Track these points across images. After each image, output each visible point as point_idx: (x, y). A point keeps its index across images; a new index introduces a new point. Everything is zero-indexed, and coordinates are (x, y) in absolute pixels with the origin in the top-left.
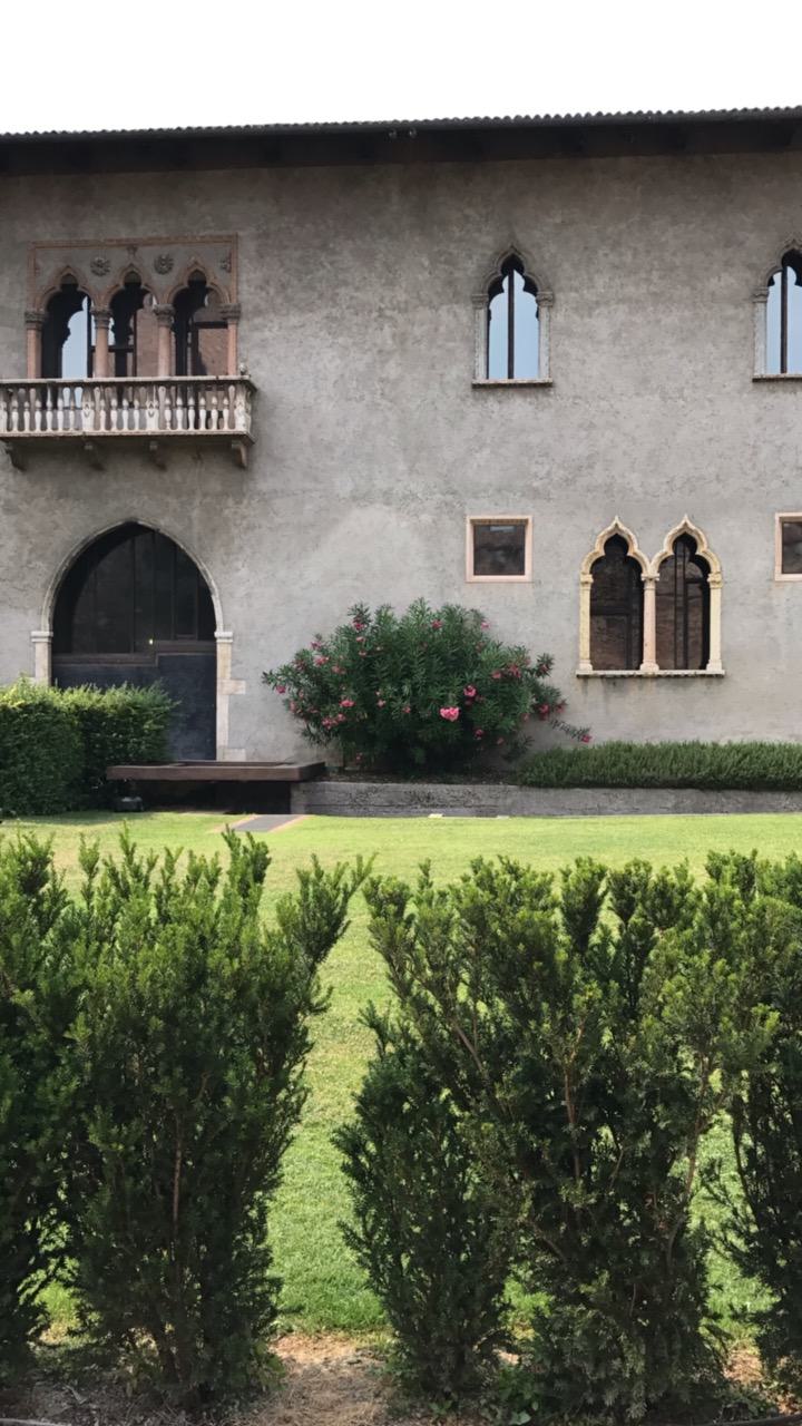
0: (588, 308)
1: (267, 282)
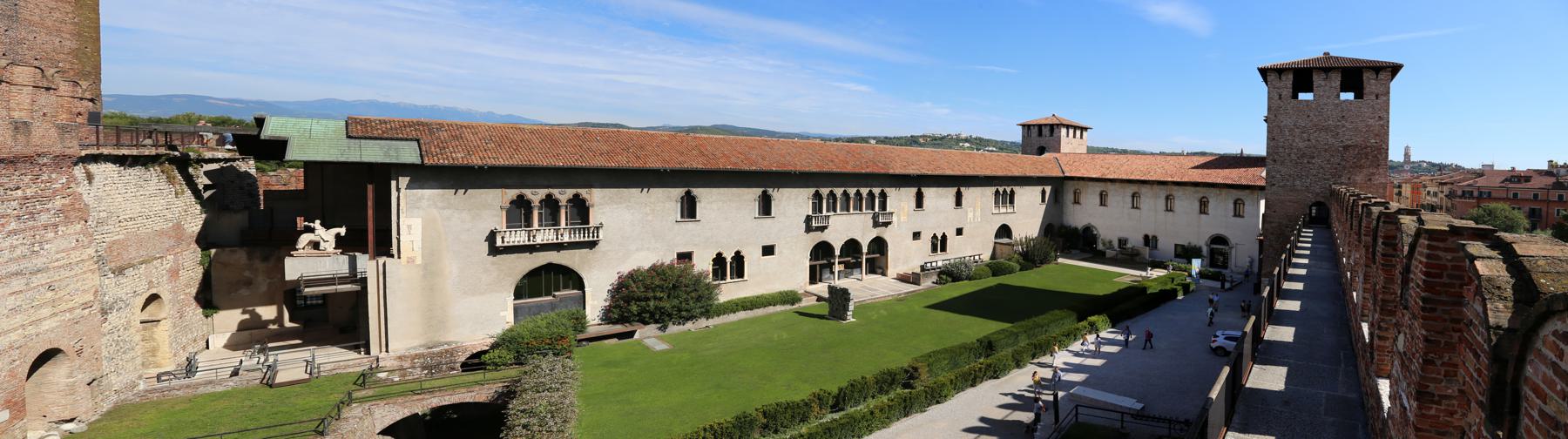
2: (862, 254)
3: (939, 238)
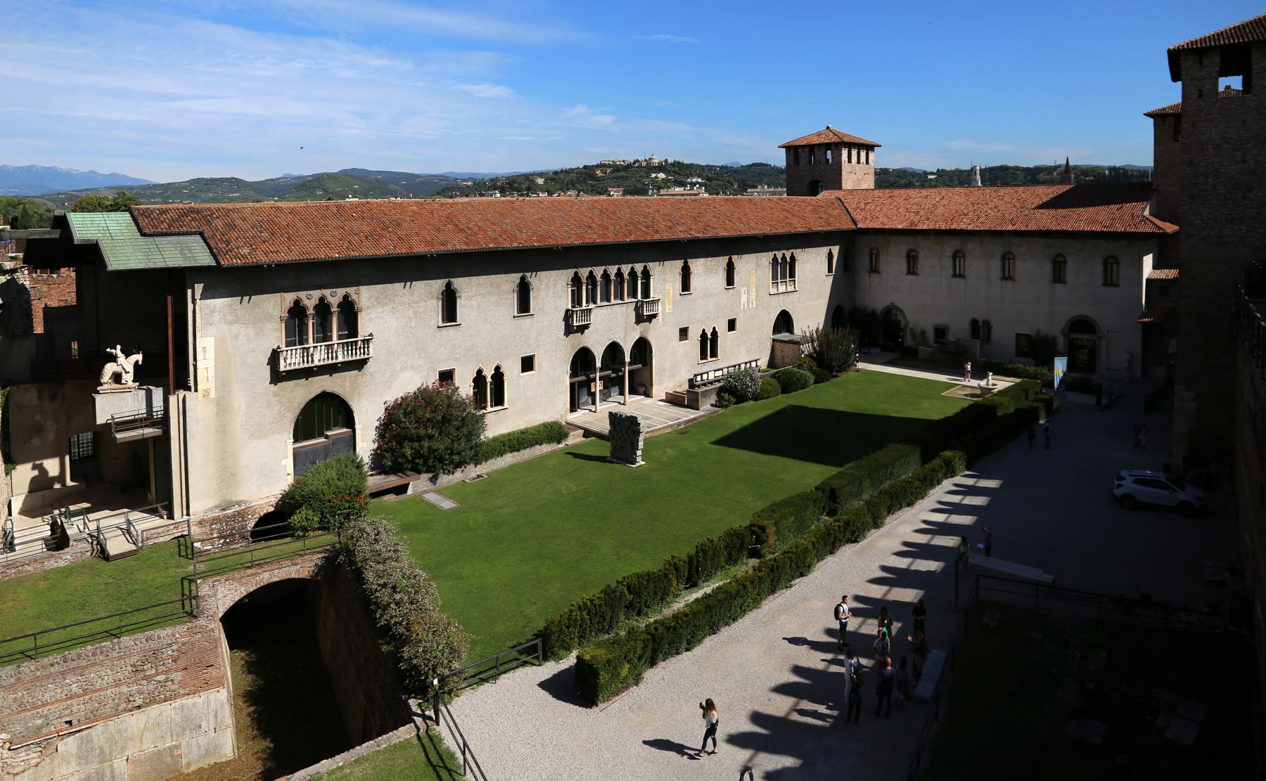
0: (470, 298)
1: (371, 297)
2: (623, 363)
3: (709, 336)
